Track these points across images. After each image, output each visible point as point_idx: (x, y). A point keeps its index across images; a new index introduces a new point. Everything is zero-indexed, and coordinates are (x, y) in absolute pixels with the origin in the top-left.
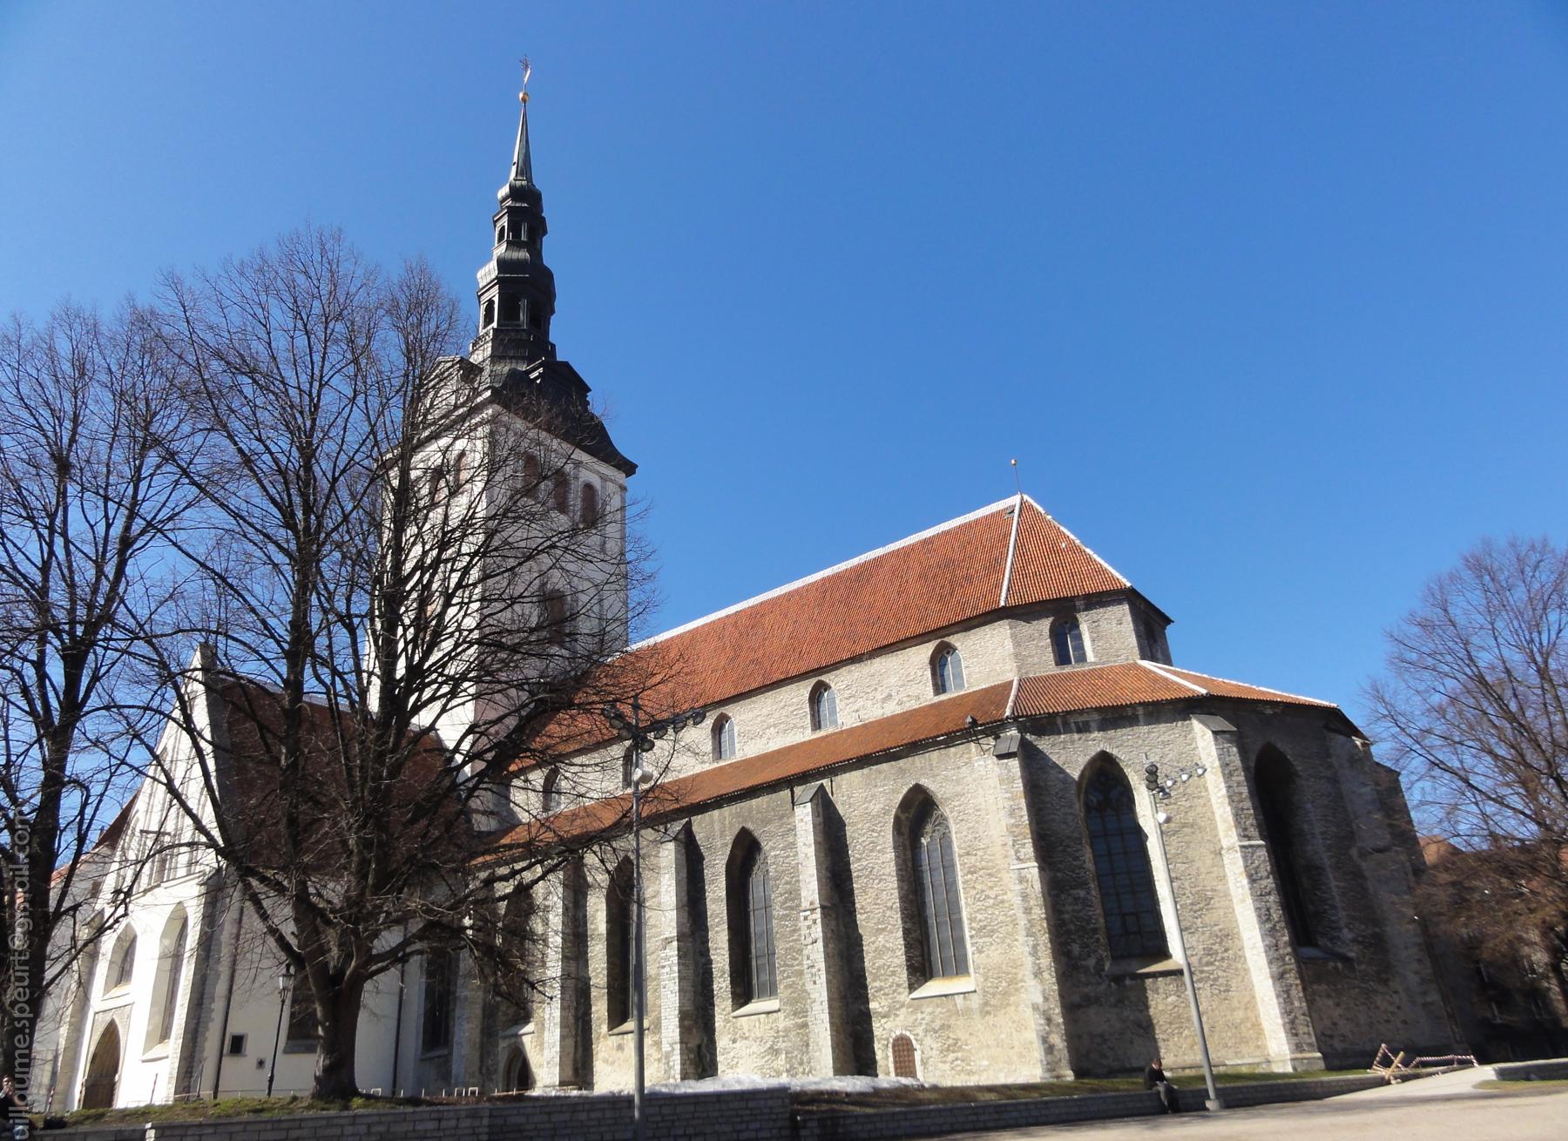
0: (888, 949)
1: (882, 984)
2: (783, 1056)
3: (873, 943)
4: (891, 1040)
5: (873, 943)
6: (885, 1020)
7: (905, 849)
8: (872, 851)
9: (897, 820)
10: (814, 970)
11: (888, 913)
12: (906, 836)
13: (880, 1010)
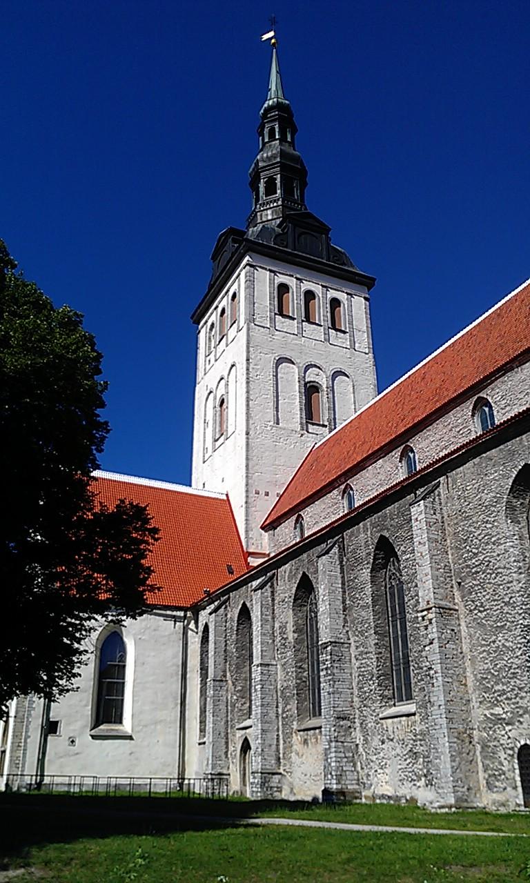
0: (508, 648)
1: (505, 687)
2: (421, 760)
3: (494, 642)
4: (516, 750)
5: (494, 642)
6: (508, 728)
7: (521, 538)
8: (487, 544)
9: (510, 508)
10: (432, 672)
11: (506, 609)
12: (524, 524)
13: (504, 716)
